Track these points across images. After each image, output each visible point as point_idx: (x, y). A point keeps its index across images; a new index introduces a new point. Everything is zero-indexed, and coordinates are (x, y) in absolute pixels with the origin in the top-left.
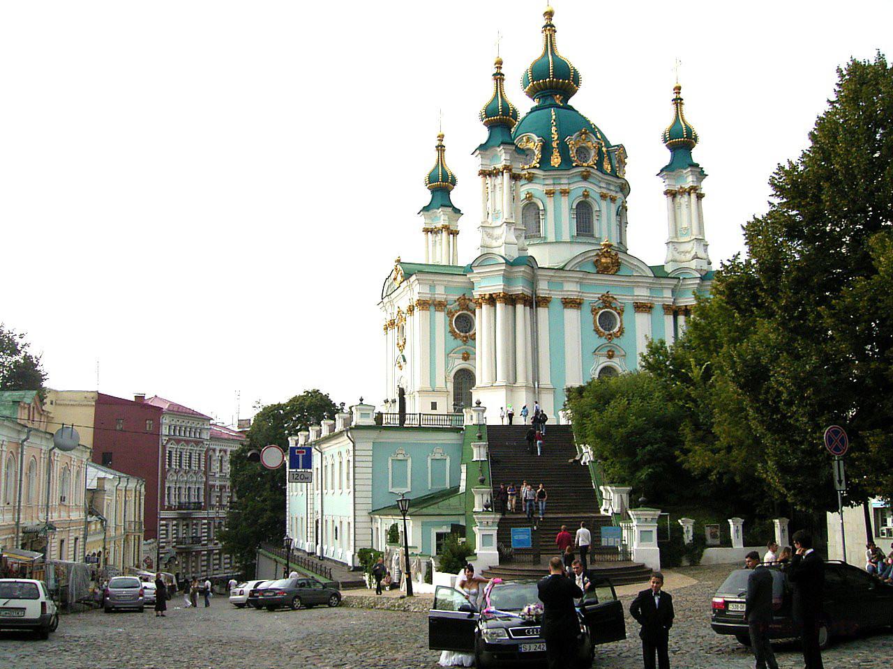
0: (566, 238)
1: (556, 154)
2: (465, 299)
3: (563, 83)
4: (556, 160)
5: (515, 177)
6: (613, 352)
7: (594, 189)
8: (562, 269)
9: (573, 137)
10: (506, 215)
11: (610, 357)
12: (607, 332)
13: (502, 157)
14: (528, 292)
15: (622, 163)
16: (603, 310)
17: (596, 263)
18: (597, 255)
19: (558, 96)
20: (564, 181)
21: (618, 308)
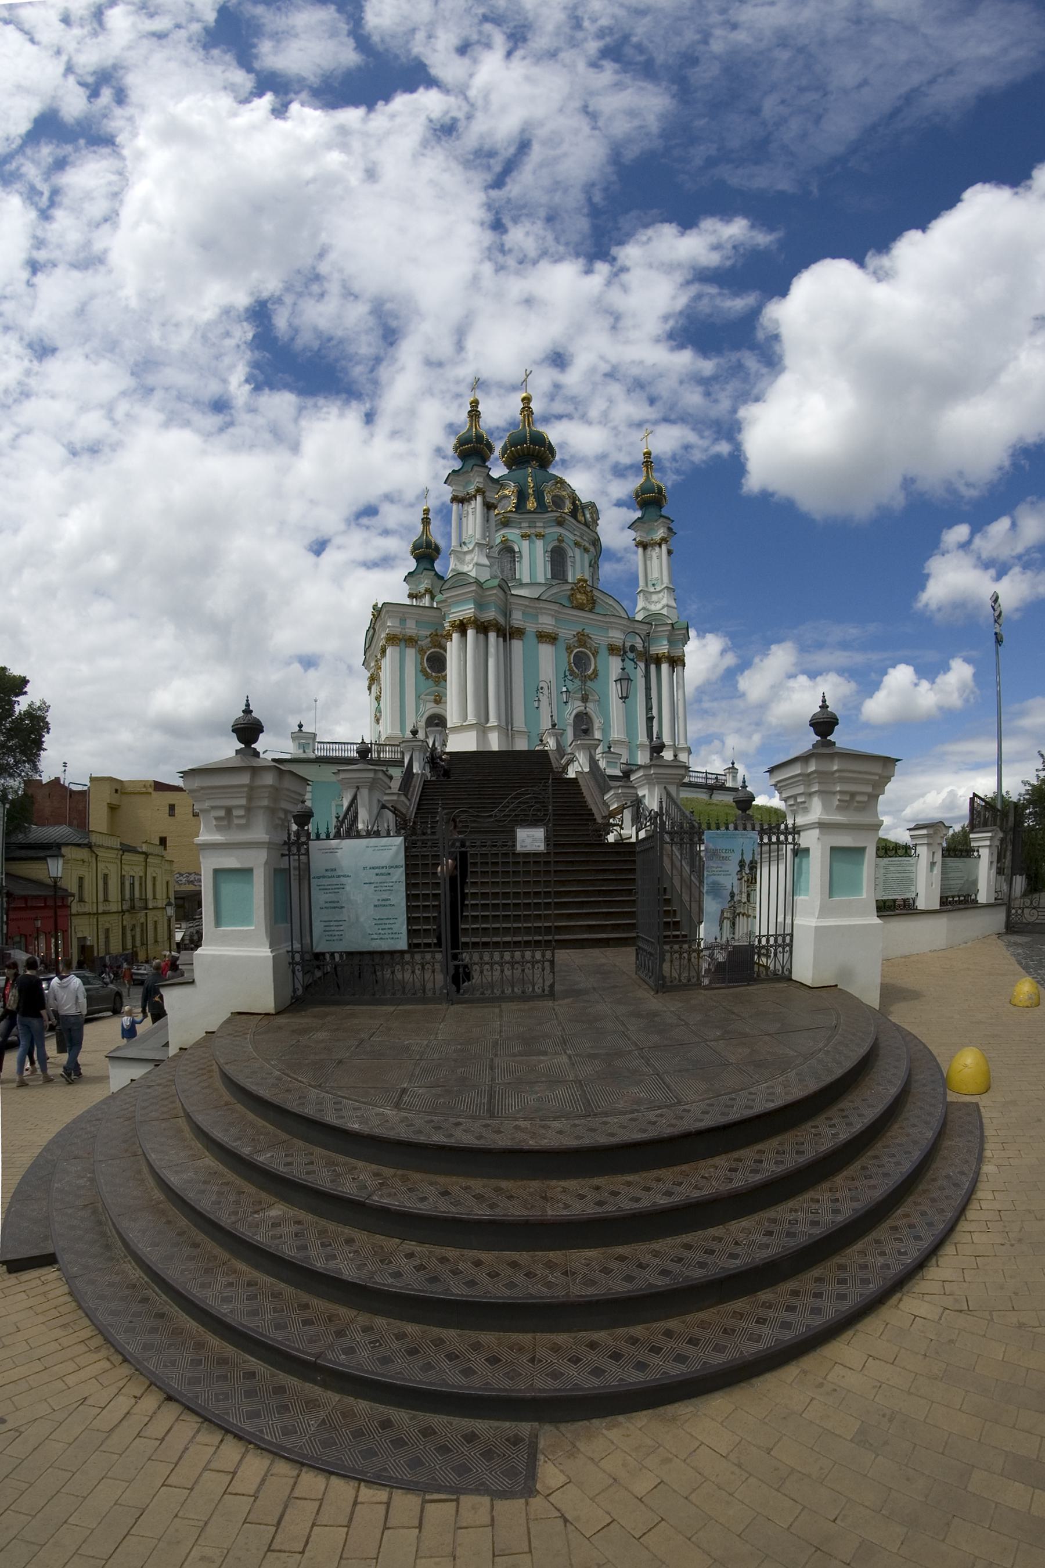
0: (541, 579)
1: (532, 498)
2: (437, 635)
3: (539, 451)
4: (531, 504)
5: (489, 506)
7: (569, 536)
8: (537, 599)
10: (478, 536)
13: (476, 481)
14: (501, 620)
15: (595, 521)
17: (571, 597)
18: (572, 589)
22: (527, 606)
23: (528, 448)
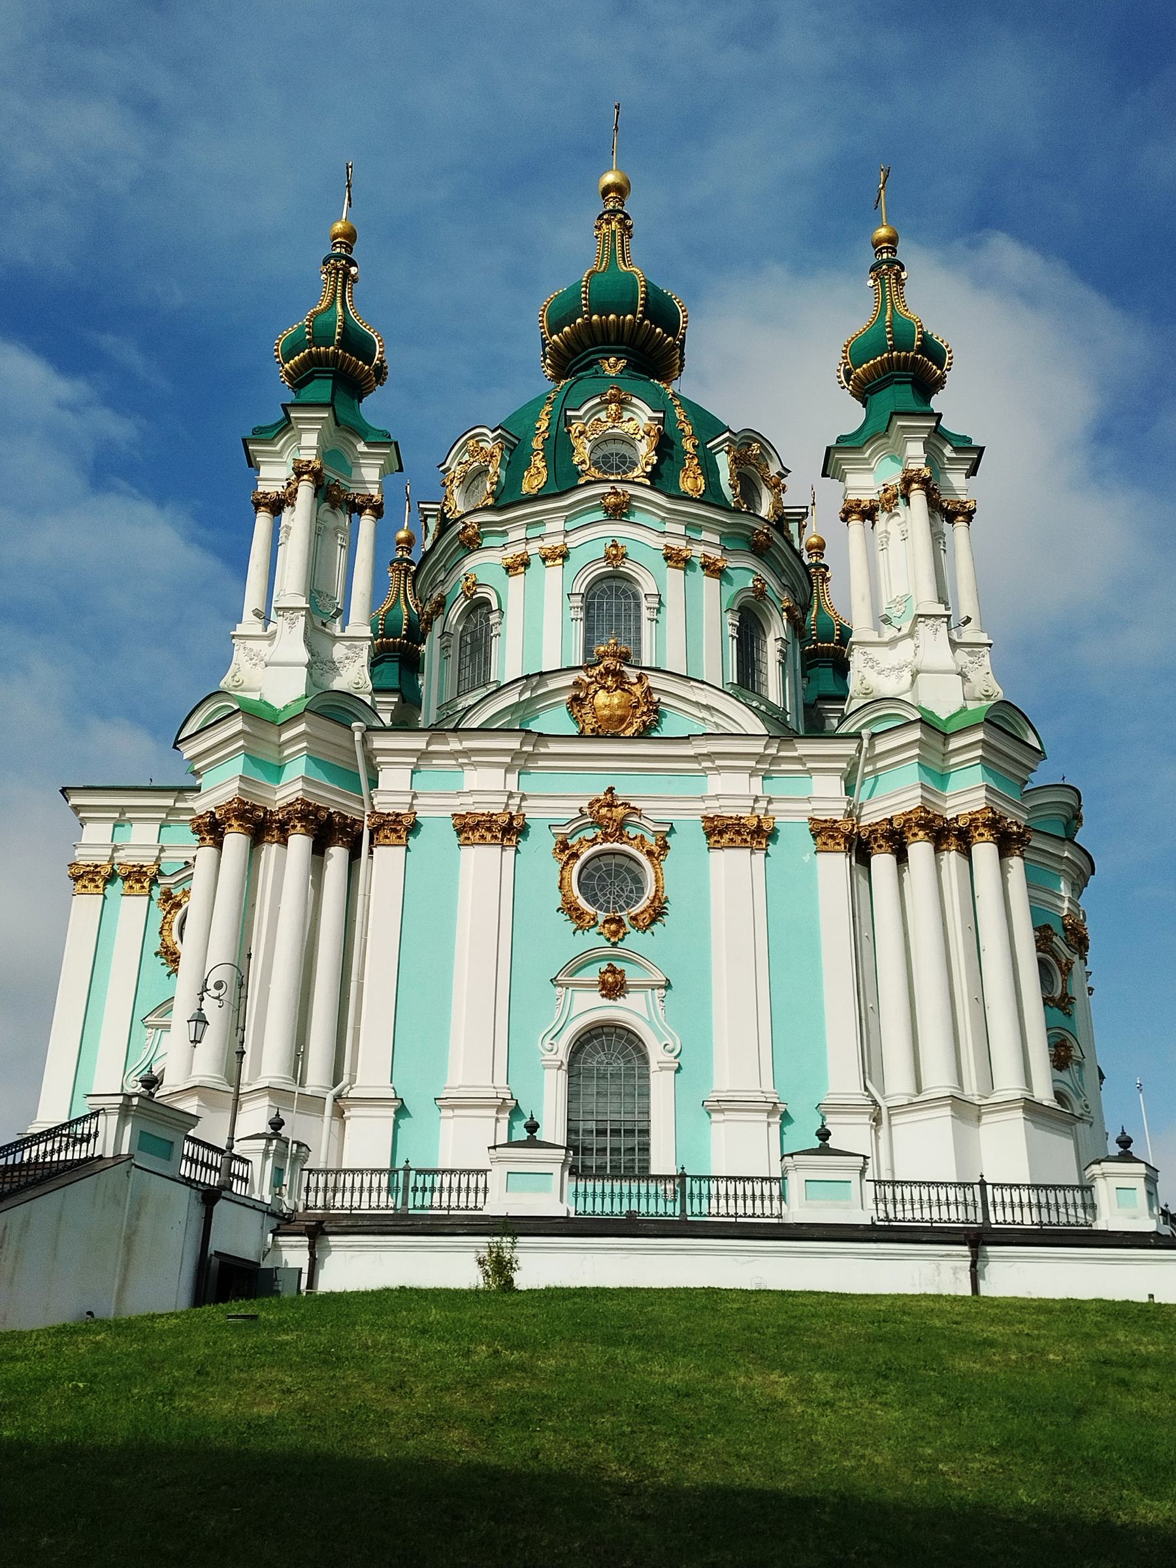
1: (538, 462)
3: (619, 326)
6: (622, 972)
7: (645, 538)
9: (580, 413)
11: (613, 987)
12: (602, 916)
16: (597, 848)
18: (577, 684)
19: (612, 360)
20: (551, 527)
21: (650, 840)
22: (423, 755)
23: (588, 324)
